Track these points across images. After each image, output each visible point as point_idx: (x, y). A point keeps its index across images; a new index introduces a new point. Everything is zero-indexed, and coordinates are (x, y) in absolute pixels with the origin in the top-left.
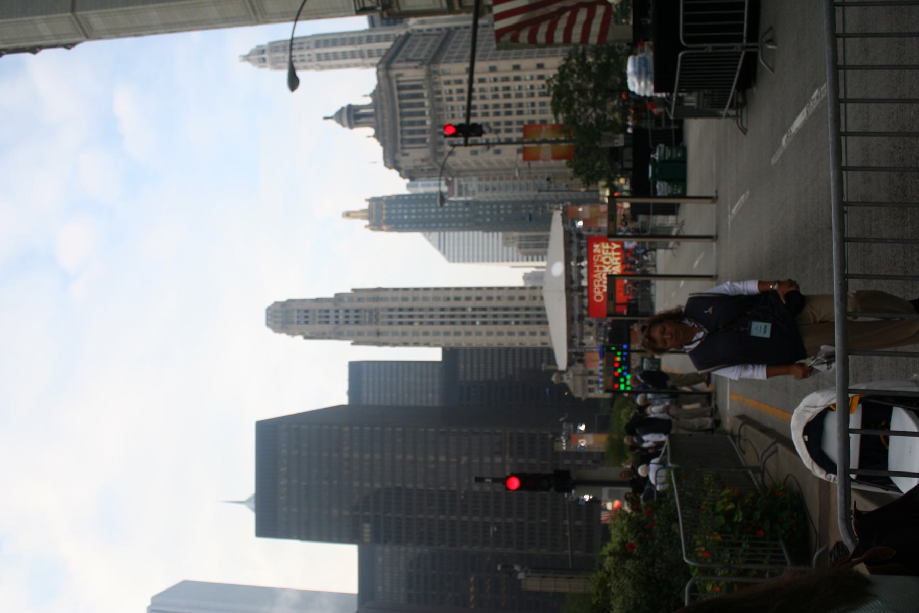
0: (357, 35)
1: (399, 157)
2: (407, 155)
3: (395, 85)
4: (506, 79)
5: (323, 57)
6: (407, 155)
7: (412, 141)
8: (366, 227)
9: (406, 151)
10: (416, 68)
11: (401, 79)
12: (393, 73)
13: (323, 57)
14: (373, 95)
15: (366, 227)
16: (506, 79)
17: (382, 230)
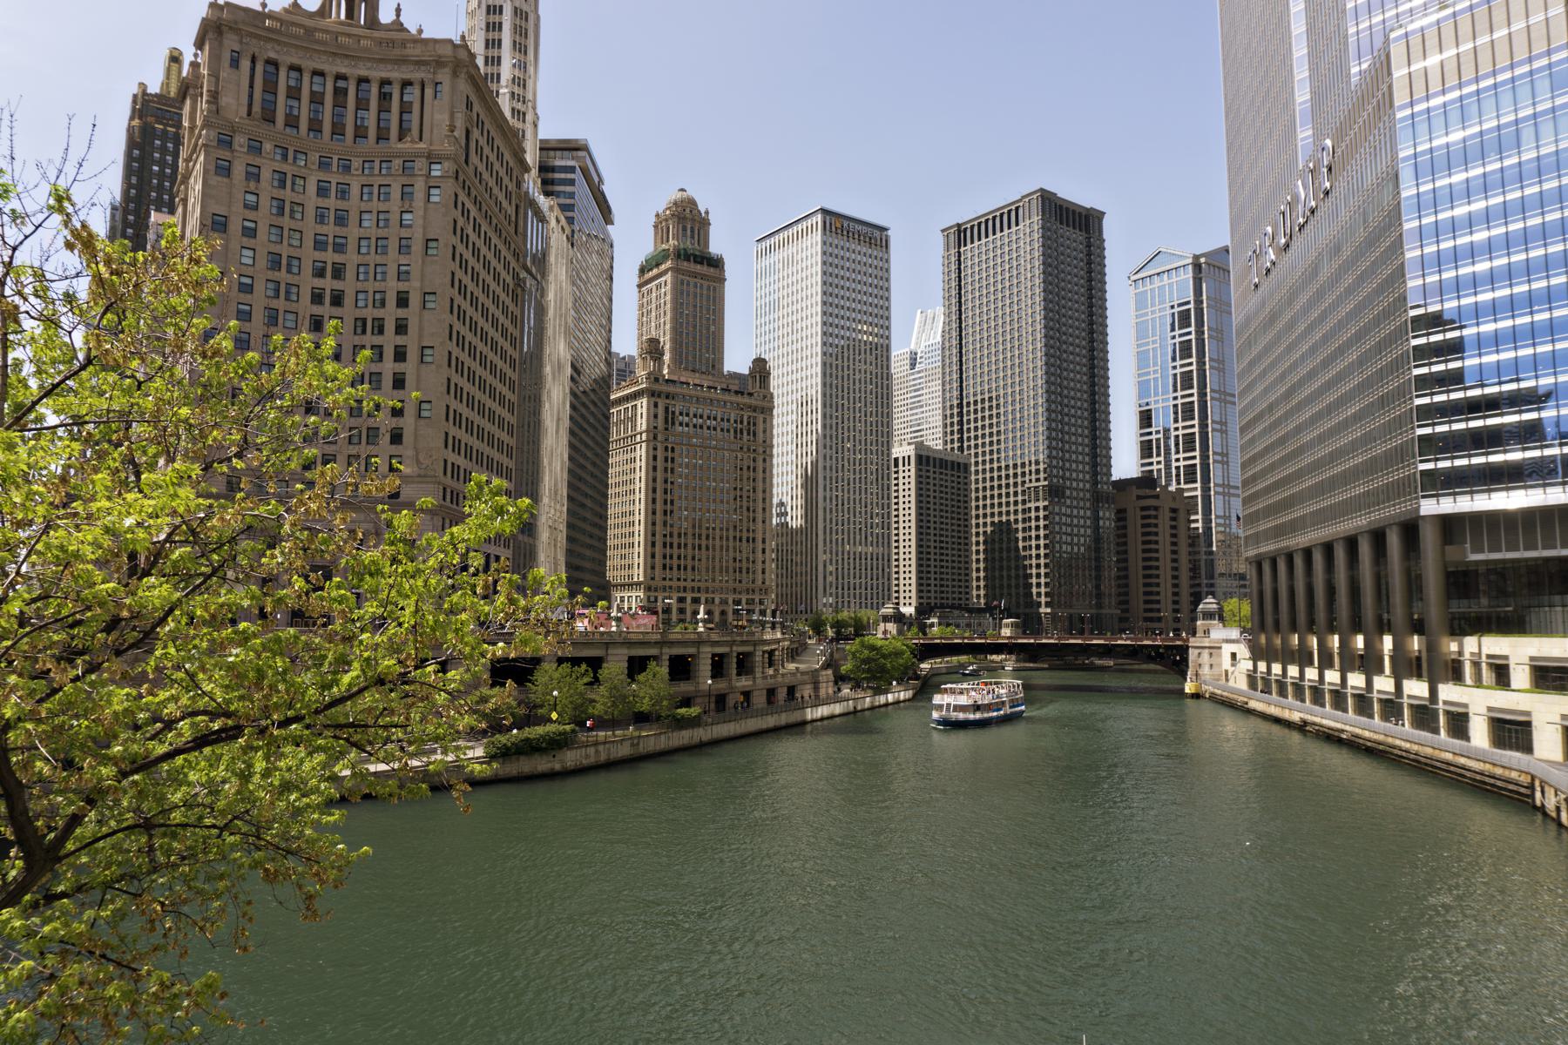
0: (529, 96)
1: (231, 42)
2: (235, 63)
3: (416, 75)
4: (401, 328)
5: (494, 18)
6: (235, 63)
7: (270, 87)
8: (143, 86)
9: (245, 64)
10: (452, 129)
11: (429, 92)
12: (444, 76)
13: (494, 18)
14: (398, 26)
15: (143, 86)
16: (401, 328)
17: (132, 118)
